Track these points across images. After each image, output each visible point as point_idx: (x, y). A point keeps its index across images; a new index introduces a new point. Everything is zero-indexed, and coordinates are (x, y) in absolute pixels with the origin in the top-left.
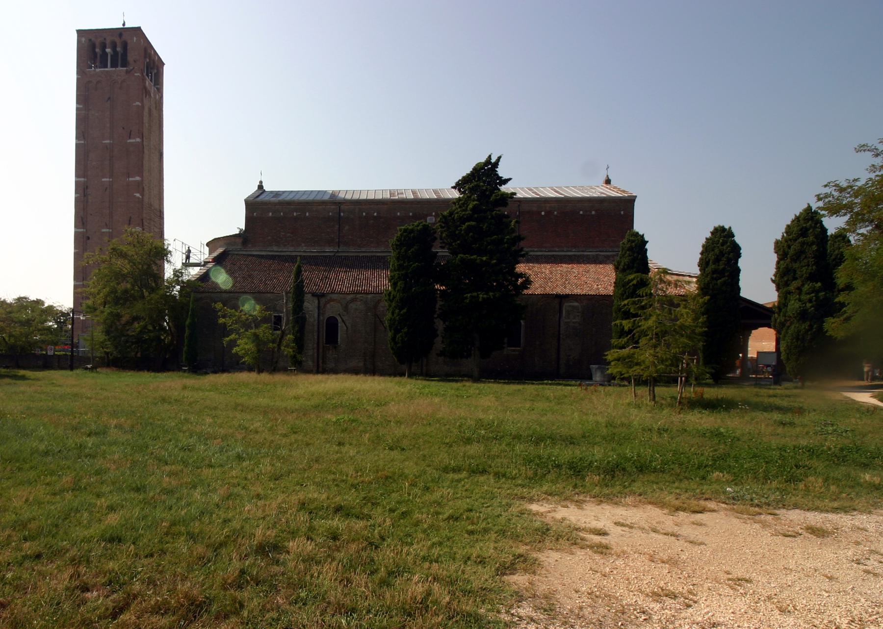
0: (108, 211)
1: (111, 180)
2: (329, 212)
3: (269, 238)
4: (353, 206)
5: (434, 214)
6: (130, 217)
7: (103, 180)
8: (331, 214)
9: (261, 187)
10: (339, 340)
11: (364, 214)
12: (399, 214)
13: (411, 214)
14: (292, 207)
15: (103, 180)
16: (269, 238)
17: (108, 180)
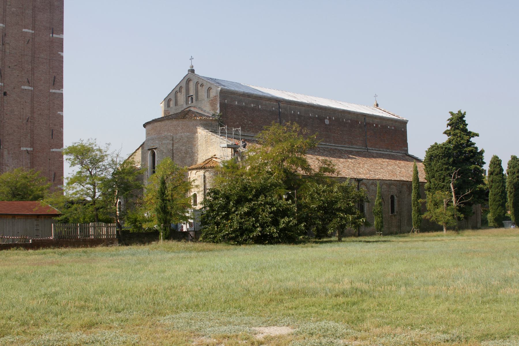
0: (30, 67)
1: (33, 32)
2: (272, 107)
3: (237, 123)
4: (286, 105)
5: (328, 118)
6: (55, 77)
7: (24, 30)
8: (274, 109)
9: (192, 71)
10: (365, 212)
11: (293, 112)
12: (310, 114)
13: (317, 116)
14: (250, 99)
15: (24, 30)
16: (237, 123)
17: (31, 31)
